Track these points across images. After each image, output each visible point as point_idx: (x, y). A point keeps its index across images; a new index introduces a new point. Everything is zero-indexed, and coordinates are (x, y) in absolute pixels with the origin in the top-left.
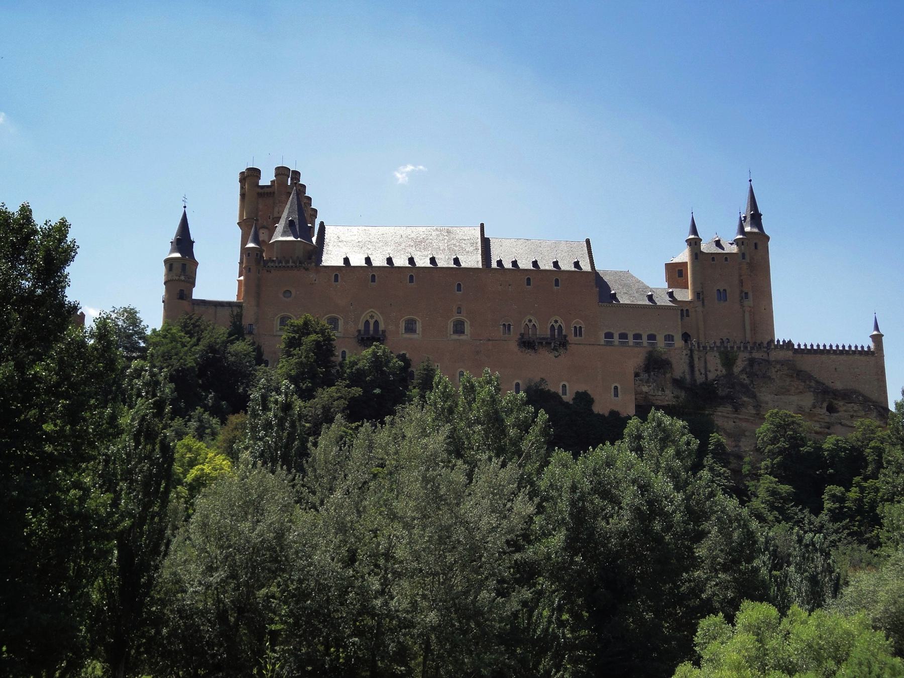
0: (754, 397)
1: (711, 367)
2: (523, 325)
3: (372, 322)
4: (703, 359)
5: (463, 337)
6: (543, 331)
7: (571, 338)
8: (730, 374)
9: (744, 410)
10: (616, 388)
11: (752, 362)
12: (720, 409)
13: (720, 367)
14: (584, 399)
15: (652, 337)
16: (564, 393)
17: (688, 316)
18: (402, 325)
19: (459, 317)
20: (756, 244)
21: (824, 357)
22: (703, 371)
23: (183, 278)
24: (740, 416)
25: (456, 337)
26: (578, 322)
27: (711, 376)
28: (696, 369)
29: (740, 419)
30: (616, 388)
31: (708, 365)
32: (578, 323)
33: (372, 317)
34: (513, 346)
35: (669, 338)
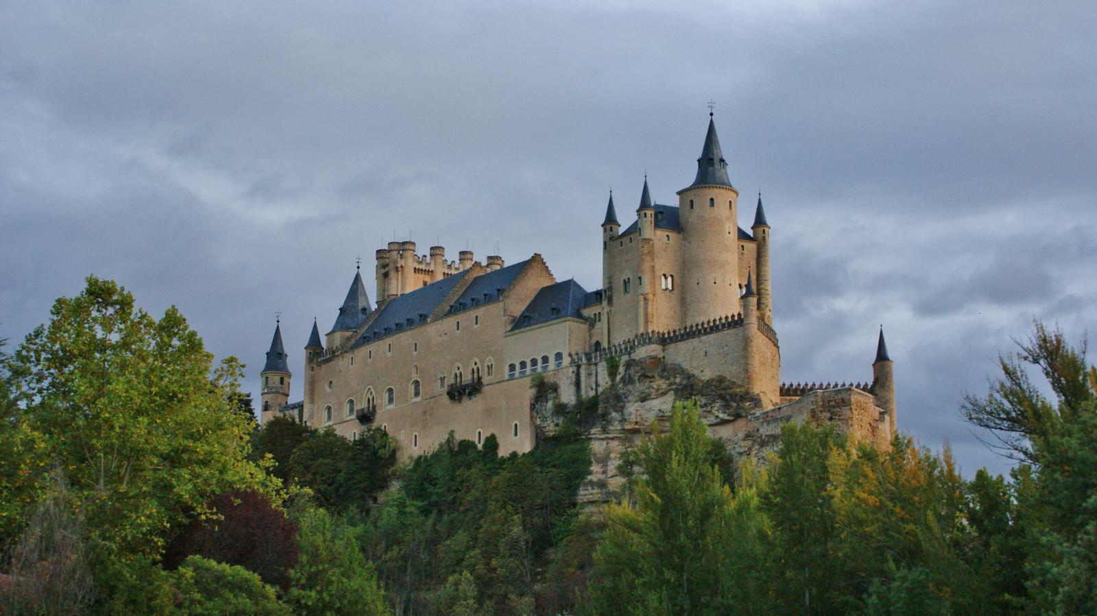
0: (621, 410)
1: (600, 382)
2: (453, 376)
3: (371, 398)
4: (594, 372)
5: (419, 399)
6: (467, 378)
7: (486, 379)
8: (613, 386)
9: (611, 428)
10: (516, 425)
11: (628, 365)
12: (593, 431)
13: (608, 379)
14: (492, 443)
15: (545, 359)
16: (479, 442)
17: (600, 320)
18: (386, 396)
19: (415, 377)
20: (692, 201)
21: (695, 342)
22: (594, 386)
23: (266, 391)
24: (610, 436)
25: (414, 400)
26: (490, 360)
27: (600, 390)
28: (583, 385)
29: (612, 439)
30: (516, 425)
31: (599, 378)
32: (490, 360)
33: (371, 393)
34: (446, 399)
35: (559, 356)
